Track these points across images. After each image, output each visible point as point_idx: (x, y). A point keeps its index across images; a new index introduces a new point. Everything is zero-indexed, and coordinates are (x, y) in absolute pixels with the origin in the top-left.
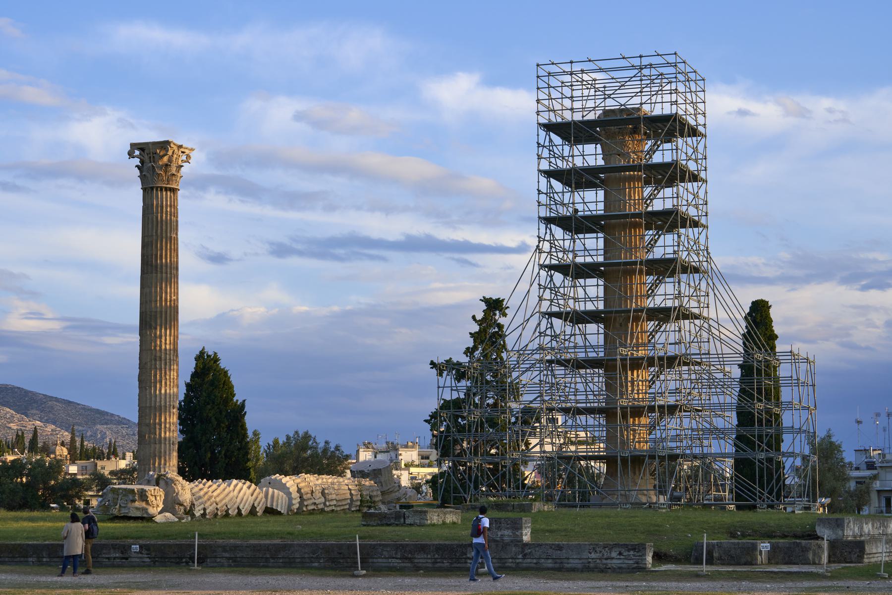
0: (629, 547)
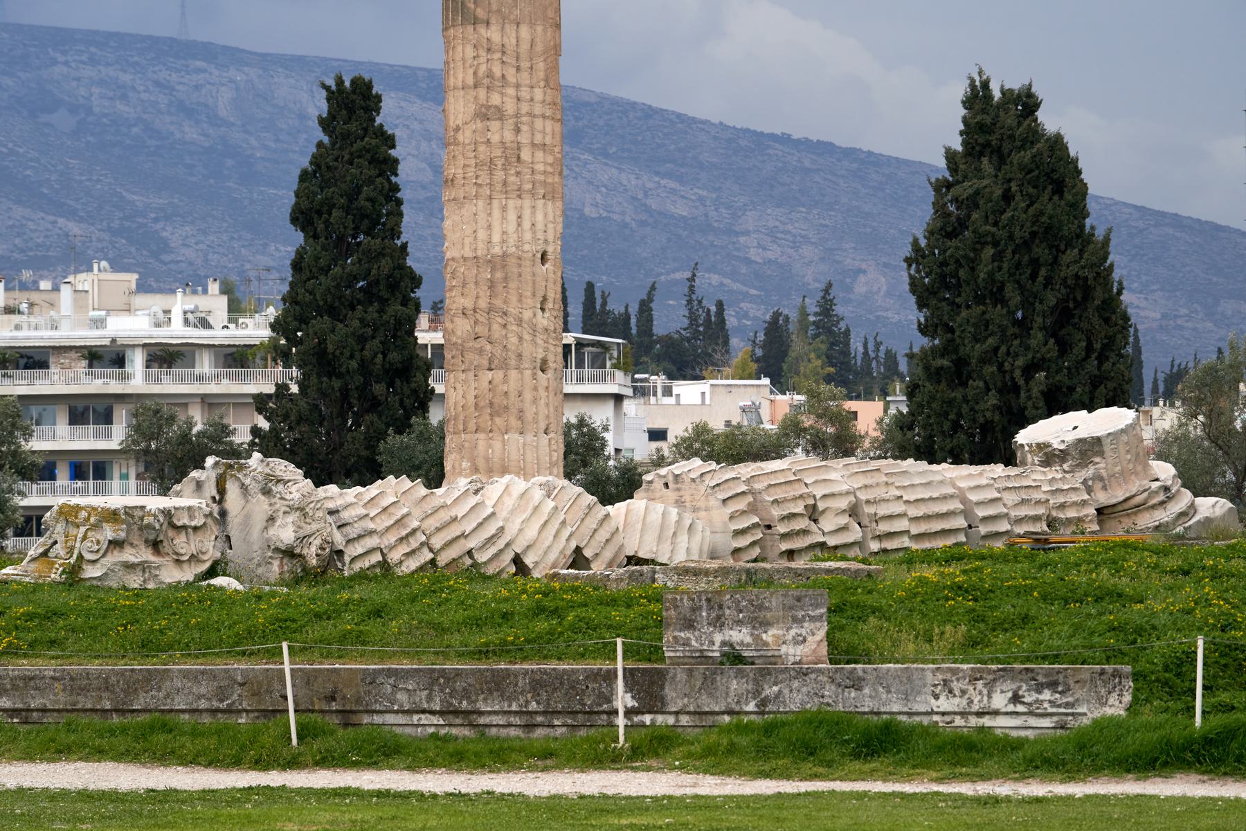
0: (1041, 679)
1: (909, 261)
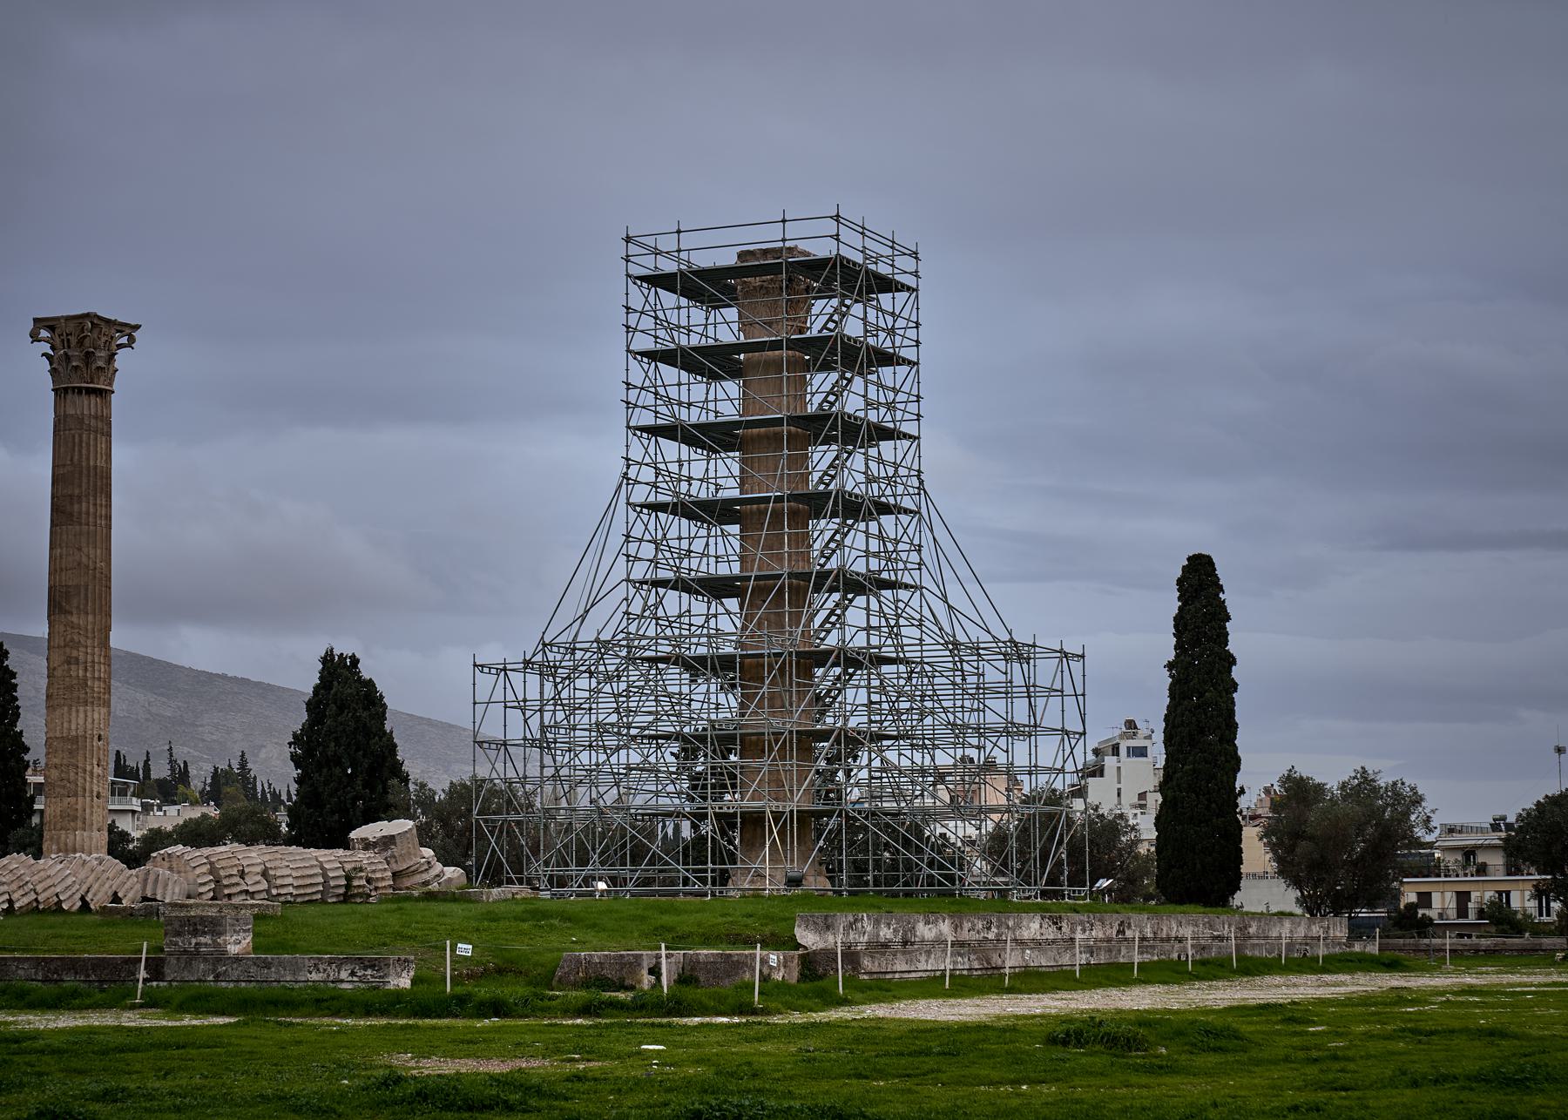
1: (290, 744)
